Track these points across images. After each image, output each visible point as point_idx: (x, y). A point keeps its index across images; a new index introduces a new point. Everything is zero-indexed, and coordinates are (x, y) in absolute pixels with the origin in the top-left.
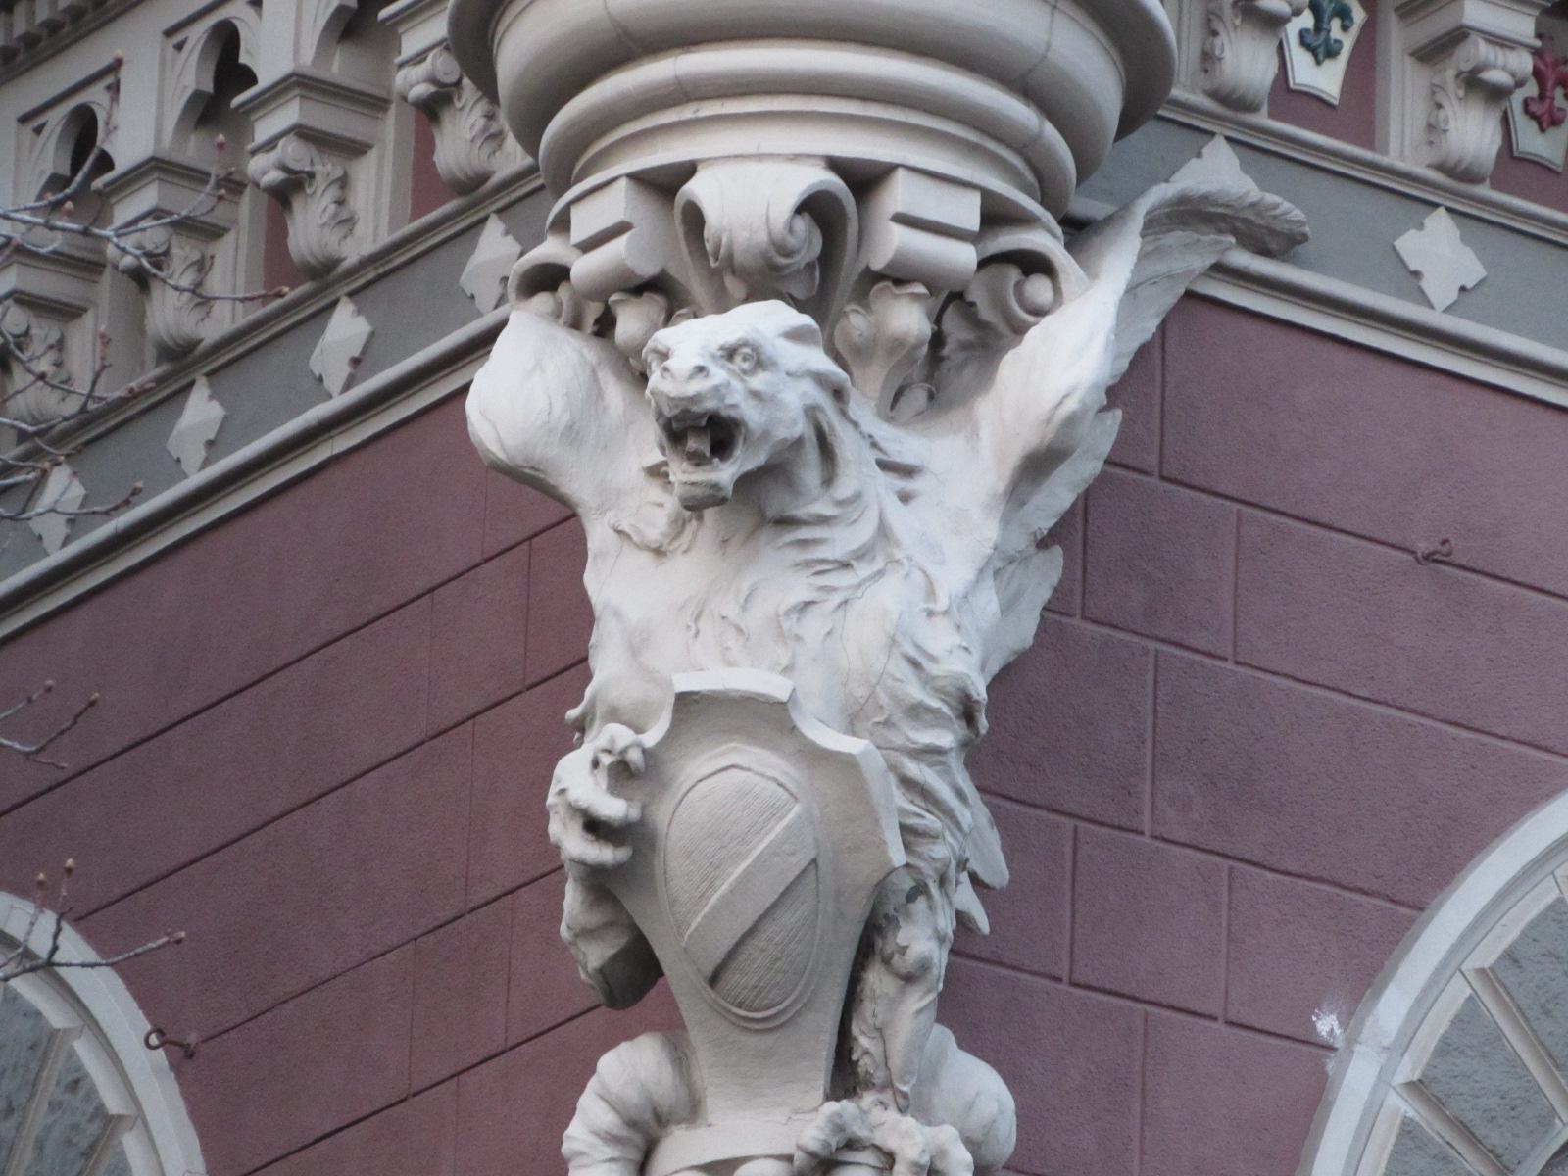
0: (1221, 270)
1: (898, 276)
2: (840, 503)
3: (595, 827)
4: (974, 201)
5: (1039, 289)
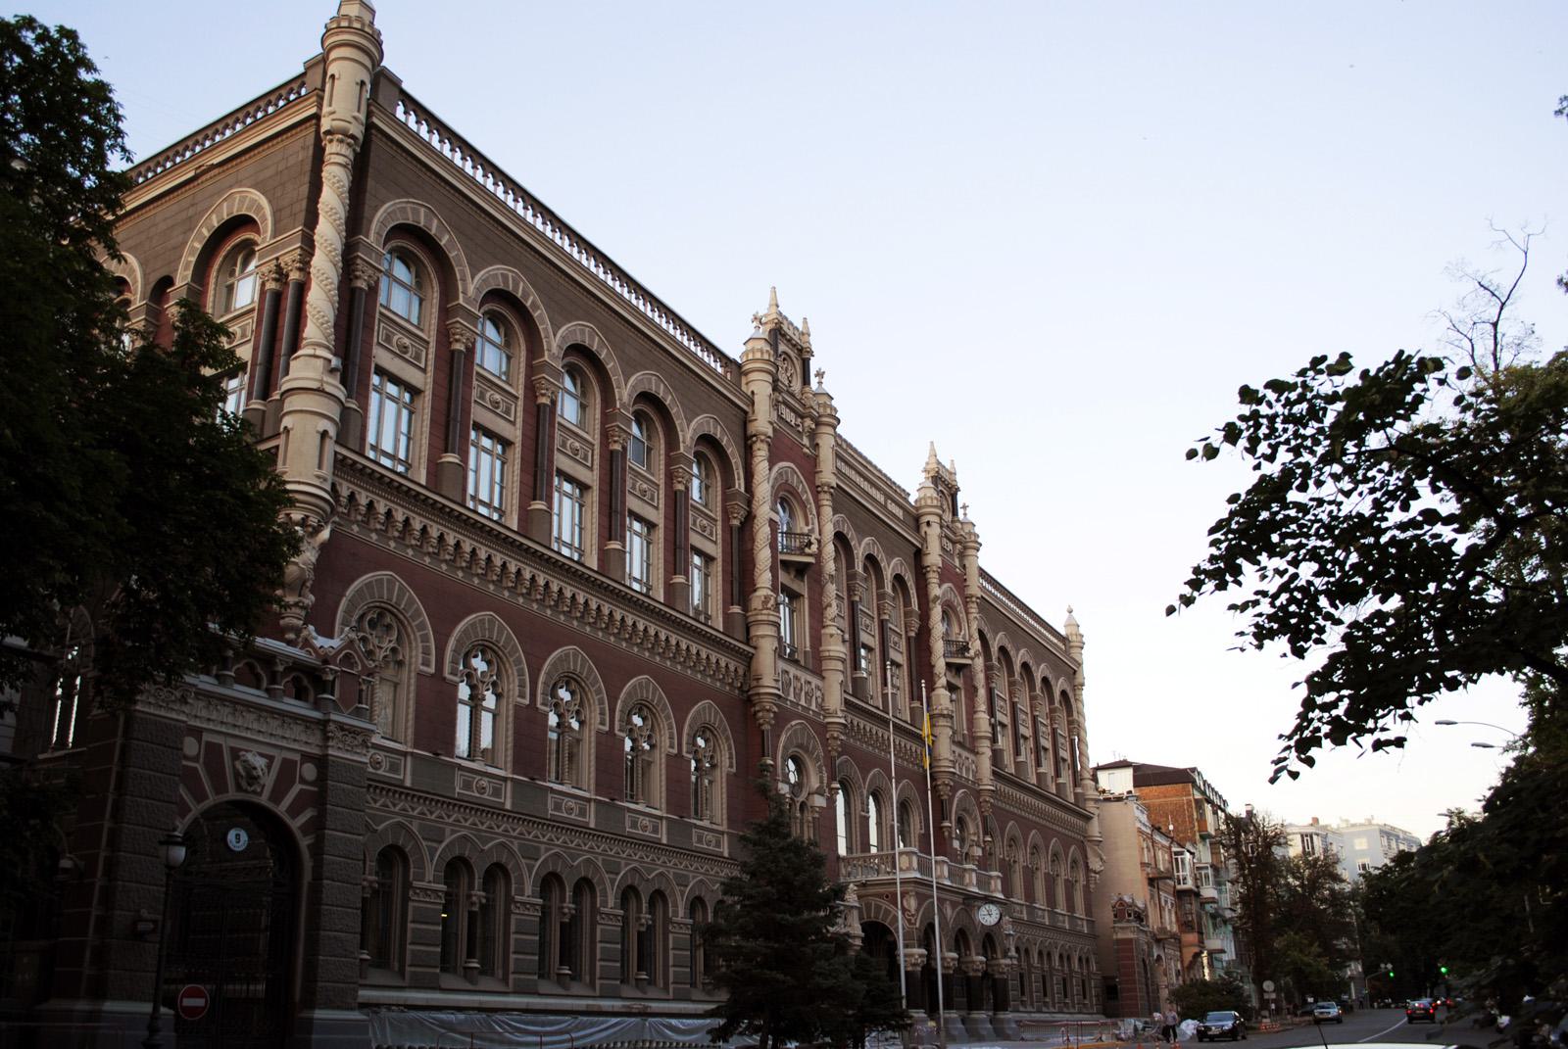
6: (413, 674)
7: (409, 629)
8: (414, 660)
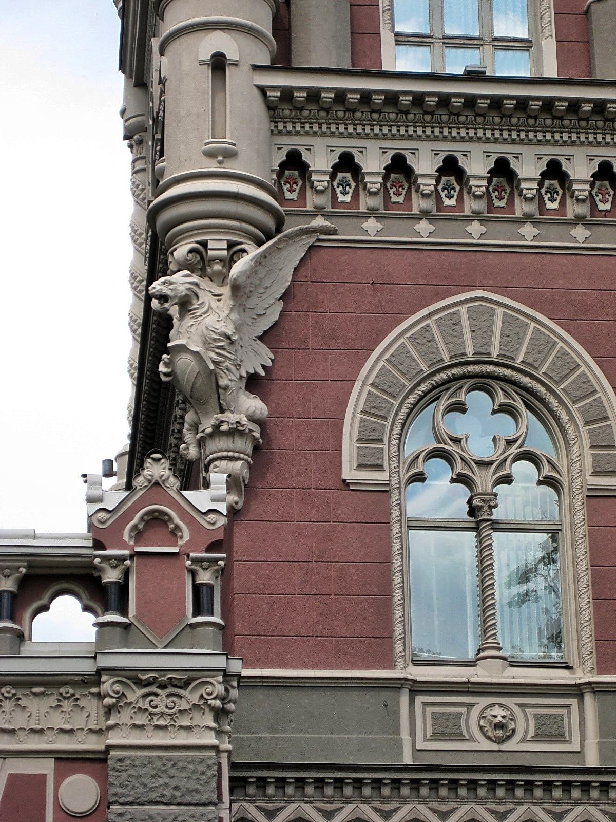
0: (318, 240)
1: (213, 260)
2: (199, 305)
3: (166, 374)
4: (226, 242)
5: (245, 254)
6: (579, 500)
7: (554, 402)
8: (576, 468)
